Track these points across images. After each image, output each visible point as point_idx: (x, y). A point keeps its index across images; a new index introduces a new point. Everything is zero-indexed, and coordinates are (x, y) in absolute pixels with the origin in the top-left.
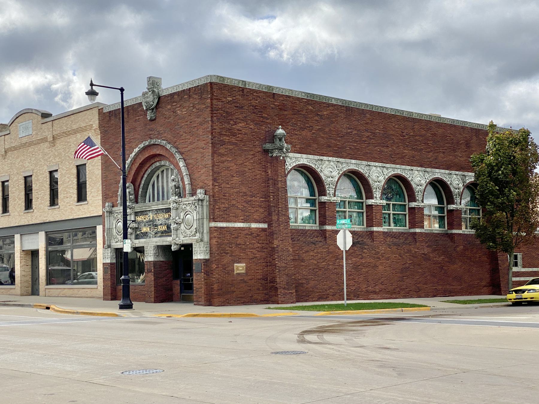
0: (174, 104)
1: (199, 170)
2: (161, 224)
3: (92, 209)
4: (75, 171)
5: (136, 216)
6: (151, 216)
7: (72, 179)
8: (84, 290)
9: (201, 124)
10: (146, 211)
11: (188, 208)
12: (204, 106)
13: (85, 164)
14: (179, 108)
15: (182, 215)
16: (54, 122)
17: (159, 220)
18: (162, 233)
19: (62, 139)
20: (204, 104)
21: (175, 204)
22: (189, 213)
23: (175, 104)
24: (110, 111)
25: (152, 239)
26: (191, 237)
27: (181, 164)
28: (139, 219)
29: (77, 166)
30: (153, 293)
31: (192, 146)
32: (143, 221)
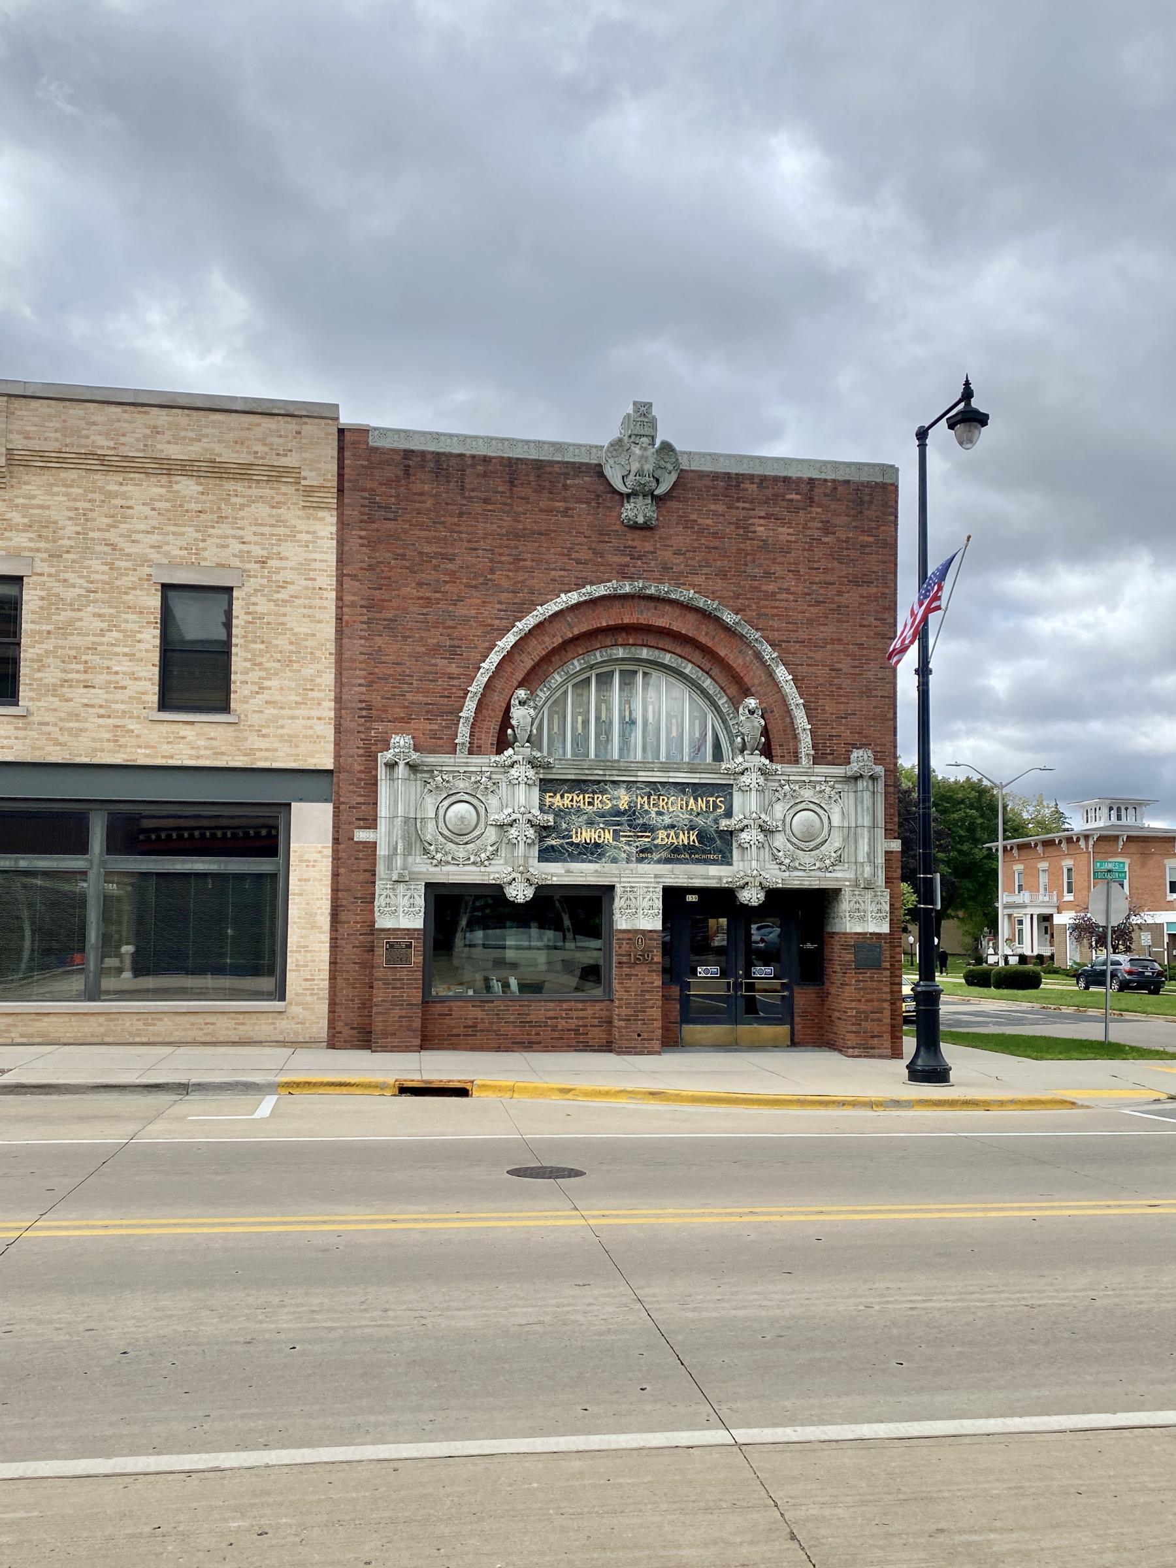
0: (738, 504)
1: (843, 699)
2: (673, 827)
3: (261, 743)
4: (154, 602)
5: (543, 791)
6: (623, 798)
7: (130, 626)
8: (193, 1019)
9: (856, 582)
10: (599, 782)
11: (807, 794)
12: (871, 539)
13: (230, 590)
14: (762, 521)
15: (779, 810)
16: (17, 403)
17: (659, 813)
18: (676, 850)
19: (73, 475)
20: (869, 532)
21: (762, 778)
22: (812, 806)
23: (747, 505)
24: (408, 454)
25: (623, 865)
26: (822, 874)
27: (782, 674)
28: (557, 801)
29: (166, 588)
30: (658, 1024)
31: (815, 632)
32: (579, 810)
